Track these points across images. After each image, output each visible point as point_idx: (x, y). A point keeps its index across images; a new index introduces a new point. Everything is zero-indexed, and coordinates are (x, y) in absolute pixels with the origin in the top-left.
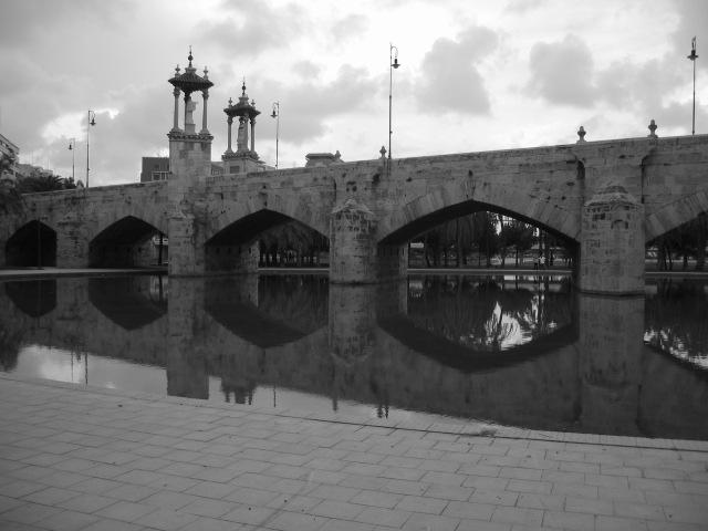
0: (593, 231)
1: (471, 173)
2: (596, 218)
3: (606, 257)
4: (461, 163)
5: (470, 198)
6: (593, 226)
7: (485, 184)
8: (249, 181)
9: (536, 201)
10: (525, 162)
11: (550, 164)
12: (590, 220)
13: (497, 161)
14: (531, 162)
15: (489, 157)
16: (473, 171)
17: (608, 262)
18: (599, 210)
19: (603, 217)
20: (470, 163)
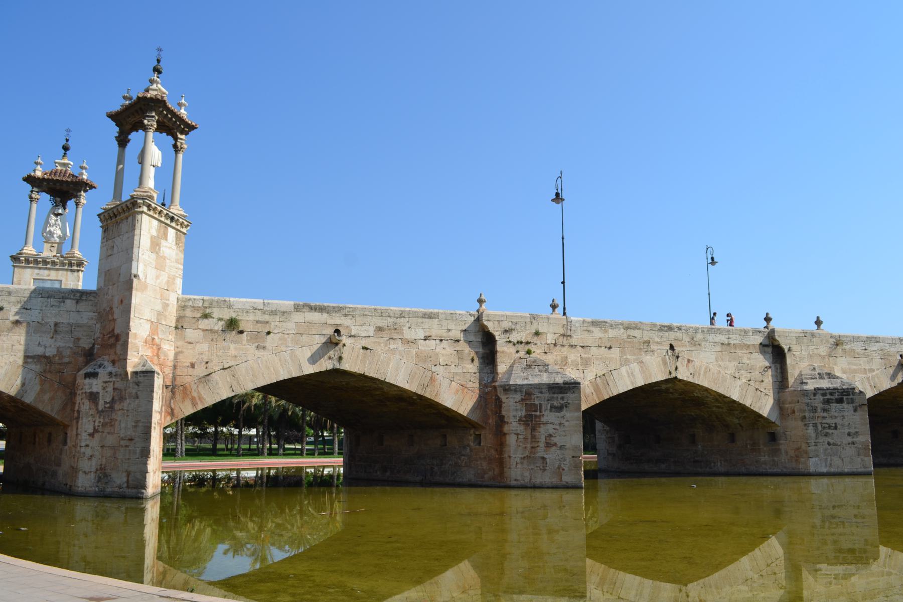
0: (825, 414)
1: (672, 347)
2: (828, 402)
3: (850, 439)
4: (661, 334)
5: (673, 375)
6: (824, 410)
7: (689, 361)
8: (298, 317)
9: (739, 383)
10: (726, 341)
11: (748, 346)
12: (820, 406)
13: (699, 336)
14: (732, 342)
15: (690, 333)
16: (674, 344)
17: (853, 443)
18: (831, 394)
19: (840, 401)
20: (671, 336)
